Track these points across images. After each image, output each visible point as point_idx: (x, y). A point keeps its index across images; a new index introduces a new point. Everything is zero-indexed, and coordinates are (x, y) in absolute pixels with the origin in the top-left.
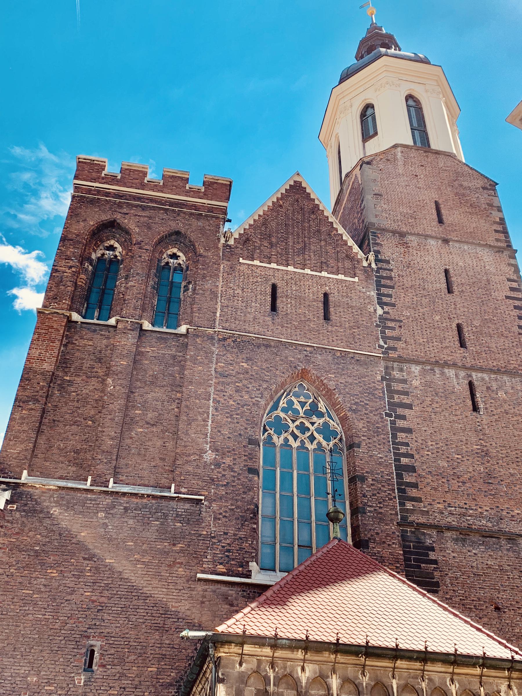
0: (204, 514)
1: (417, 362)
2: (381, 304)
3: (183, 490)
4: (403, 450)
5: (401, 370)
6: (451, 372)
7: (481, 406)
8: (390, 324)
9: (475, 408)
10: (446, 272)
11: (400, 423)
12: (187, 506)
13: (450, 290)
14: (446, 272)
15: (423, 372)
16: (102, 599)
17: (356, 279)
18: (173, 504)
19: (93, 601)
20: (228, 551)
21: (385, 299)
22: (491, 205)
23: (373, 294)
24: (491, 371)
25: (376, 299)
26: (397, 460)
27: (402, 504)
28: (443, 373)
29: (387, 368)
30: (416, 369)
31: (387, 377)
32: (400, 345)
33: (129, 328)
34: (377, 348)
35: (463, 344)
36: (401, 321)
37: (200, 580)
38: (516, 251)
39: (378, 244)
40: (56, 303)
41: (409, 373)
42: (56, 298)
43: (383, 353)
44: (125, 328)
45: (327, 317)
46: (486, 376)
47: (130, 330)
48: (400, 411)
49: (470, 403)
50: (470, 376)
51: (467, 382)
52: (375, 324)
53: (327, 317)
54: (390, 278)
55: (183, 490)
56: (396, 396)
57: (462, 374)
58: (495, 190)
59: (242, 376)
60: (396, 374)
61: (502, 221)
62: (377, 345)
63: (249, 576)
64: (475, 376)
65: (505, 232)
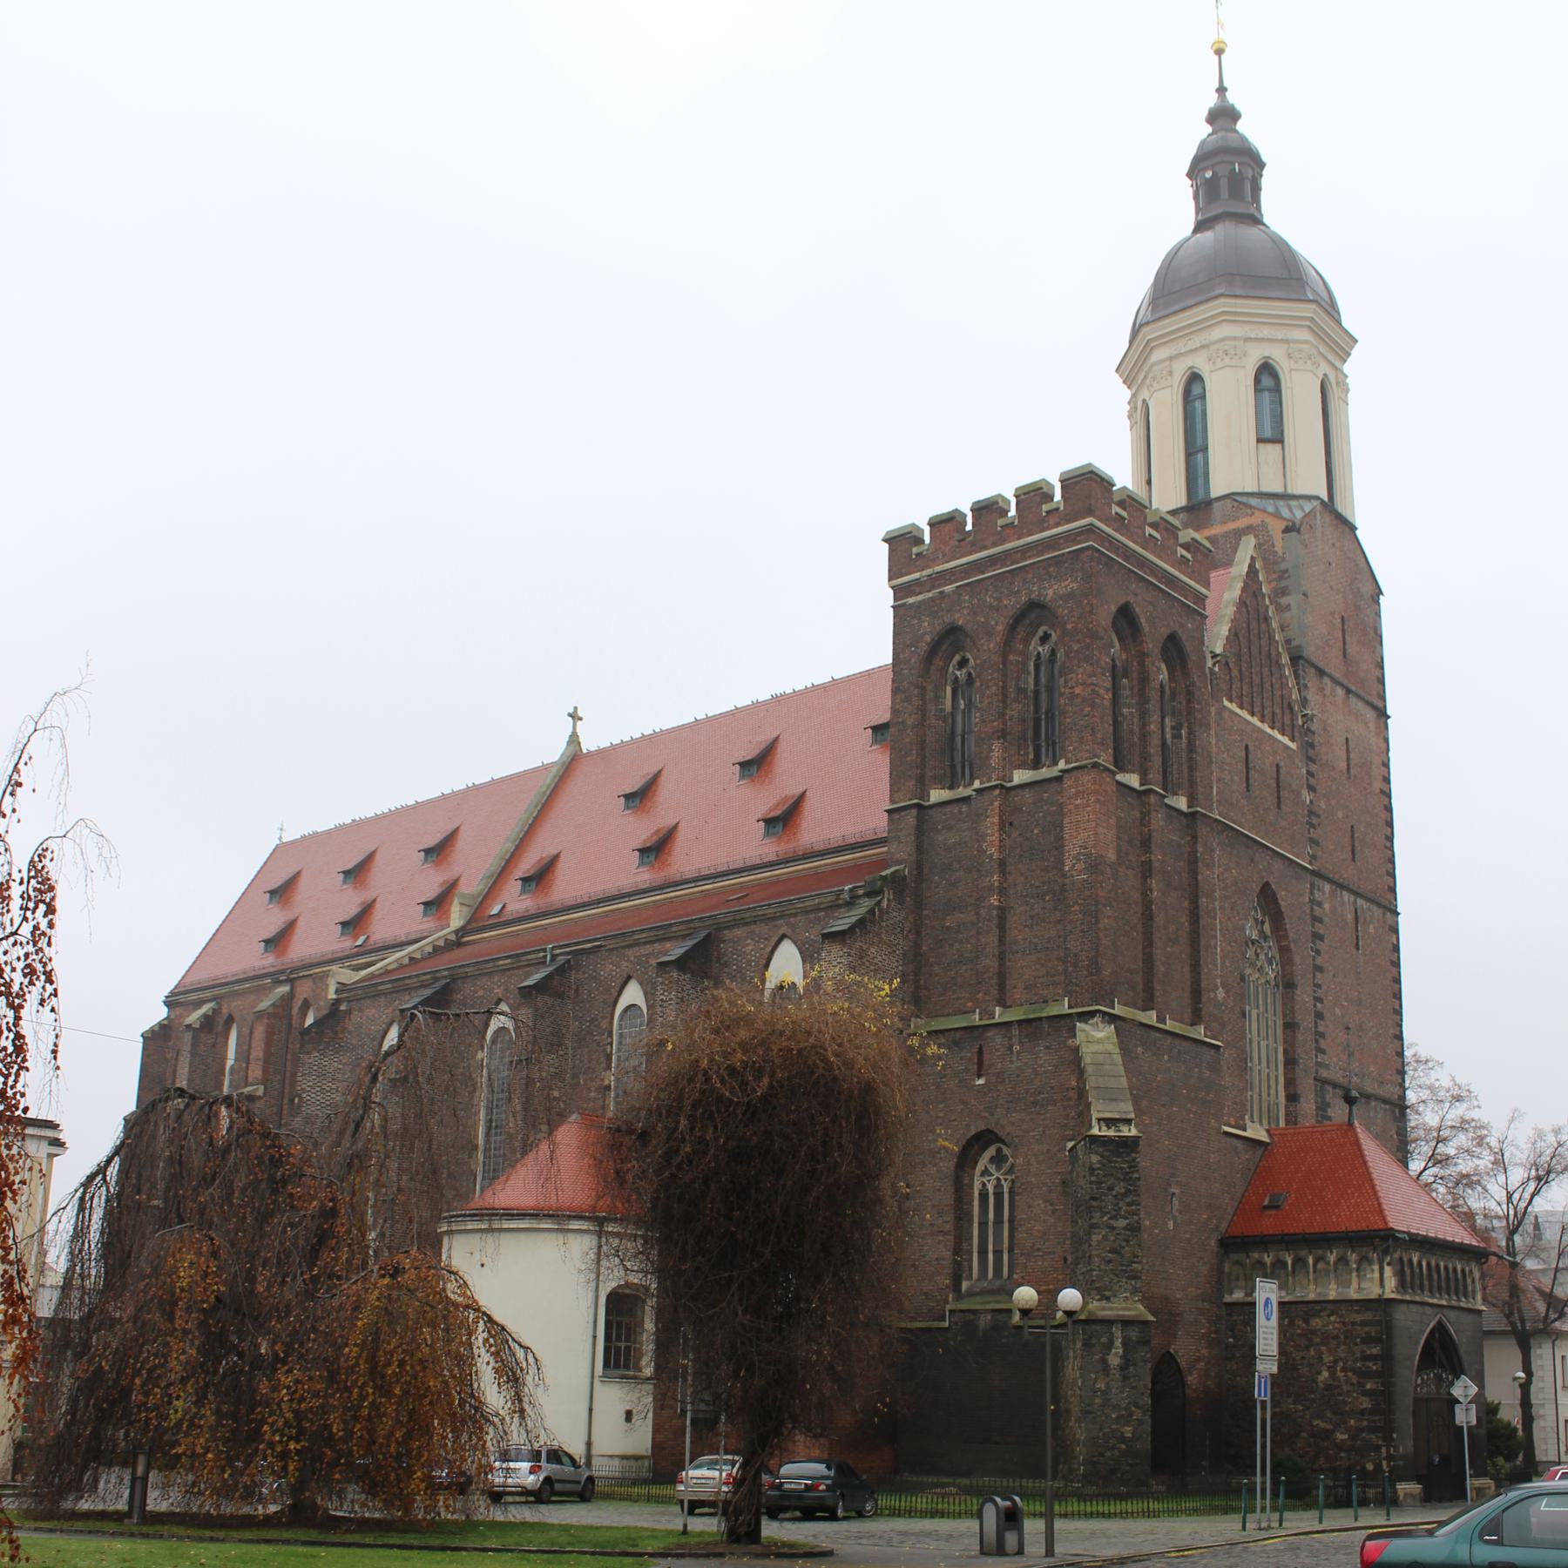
0: (1222, 1063)
2: (1311, 789)
3: (1209, 1034)
4: (1319, 993)
5: (1319, 890)
6: (1346, 895)
8: (1315, 820)
10: (1347, 739)
11: (1319, 961)
12: (1212, 1052)
14: (1347, 739)
16: (1175, 1149)
17: (1293, 746)
18: (1205, 1048)
19: (1170, 1150)
20: (1235, 1103)
21: (1312, 781)
23: (1304, 771)
26: (1315, 1006)
27: (1316, 1056)
28: (1341, 896)
30: (1327, 887)
35: (1354, 859)
36: (1319, 816)
37: (1226, 1133)
38: (1389, 717)
43: (1310, 863)
45: (1279, 807)
46: (1364, 903)
50: (1355, 902)
53: (1279, 807)
54: (1312, 745)
55: (1209, 1034)
56: (1317, 924)
57: (1352, 898)
58: (1379, 605)
59: (1233, 888)
63: (1245, 1130)
64: (1360, 901)
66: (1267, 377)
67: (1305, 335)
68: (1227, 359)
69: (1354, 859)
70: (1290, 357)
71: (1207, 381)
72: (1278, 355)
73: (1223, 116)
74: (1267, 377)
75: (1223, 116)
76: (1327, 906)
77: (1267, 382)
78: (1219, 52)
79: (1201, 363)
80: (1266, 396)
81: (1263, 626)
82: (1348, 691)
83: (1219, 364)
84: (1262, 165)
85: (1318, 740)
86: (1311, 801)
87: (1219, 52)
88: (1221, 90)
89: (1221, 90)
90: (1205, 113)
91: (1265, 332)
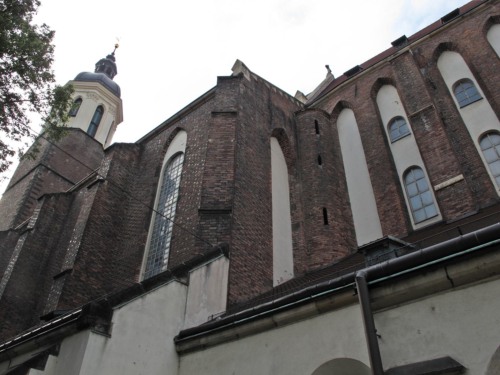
66: (100, 110)
67: (115, 106)
68: (93, 97)
70: (109, 109)
71: (82, 103)
72: (107, 107)
73: (111, 57)
74: (100, 110)
75: (111, 57)
77: (99, 110)
78: (116, 47)
79: (84, 96)
80: (98, 113)
83: (90, 97)
84: (116, 73)
87: (116, 47)
88: (113, 54)
89: (113, 54)
90: (107, 55)
91: (106, 99)
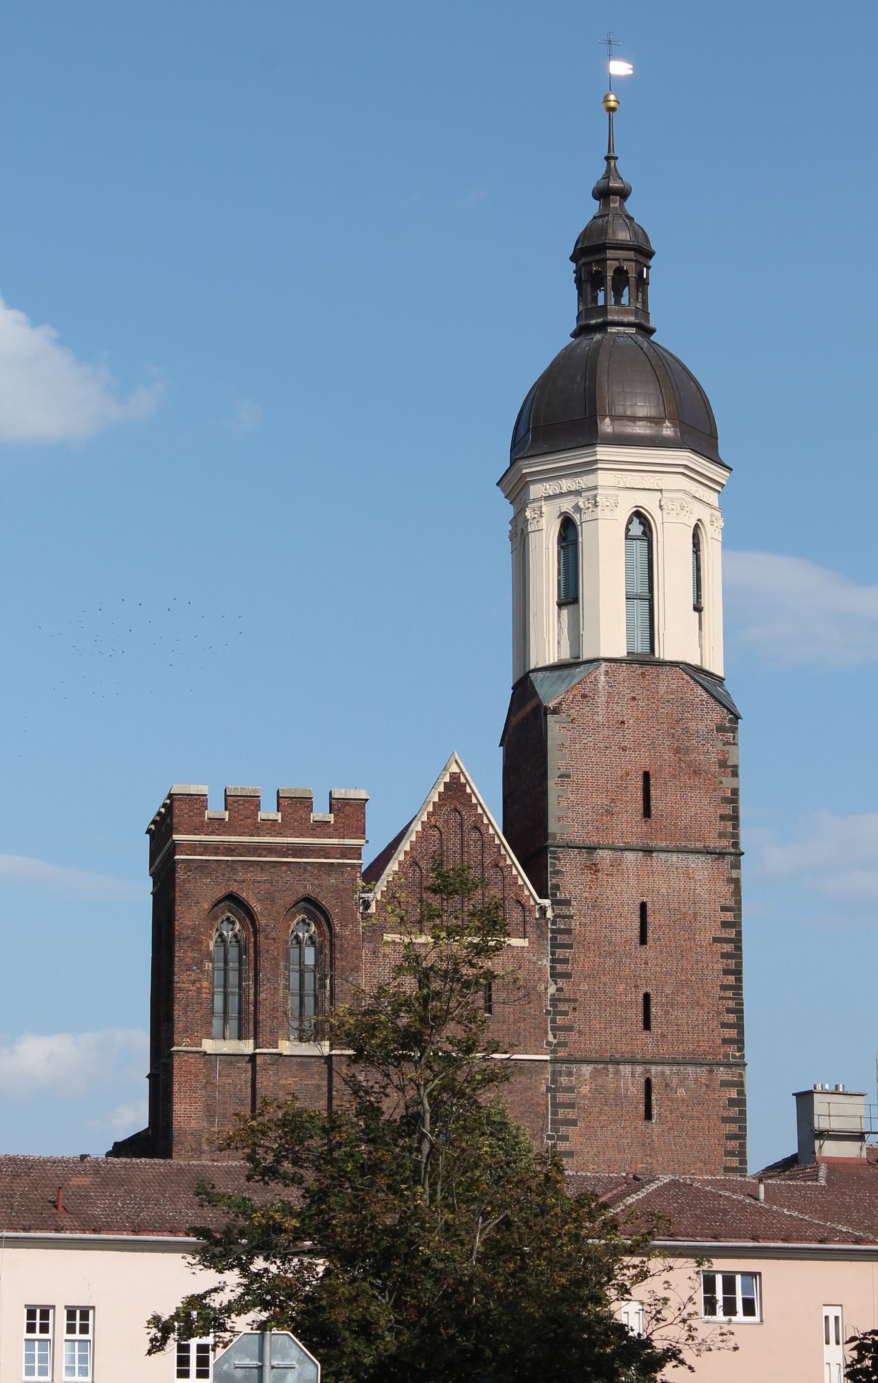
1: (589, 1062)
5: (570, 1074)
7: (655, 1111)
9: (648, 1116)
10: (643, 906)
13: (643, 940)
14: (643, 906)
15: (594, 1074)
22: (723, 764)
24: (674, 1062)
25: (549, 968)
28: (617, 1072)
29: (554, 1073)
30: (587, 1070)
31: (553, 1086)
32: (574, 1036)
33: (269, 1061)
34: (545, 1047)
35: (647, 1025)
36: (576, 1000)
39: (557, 872)
40: (188, 1037)
41: (579, 1076)
42: (187, 1031)
44: (265, 1063)
46: (667, 1069)
47: (269, 1064)
48: (563, 1130)
49: (642, 1107)
50: (648, 1071)
51: (643, 1080)
52: (544, 1011)
54: (568, 932)
56: (560, 1111)
60: (564, 1080)
61: (733, 798)
62: (545, 1041)
65: (734, 818)
69: (647, 1025)
76: (585, 1089)
81: (475, 835)
82: (648, 851)
85: (574, 924)
86: (560, 990)
